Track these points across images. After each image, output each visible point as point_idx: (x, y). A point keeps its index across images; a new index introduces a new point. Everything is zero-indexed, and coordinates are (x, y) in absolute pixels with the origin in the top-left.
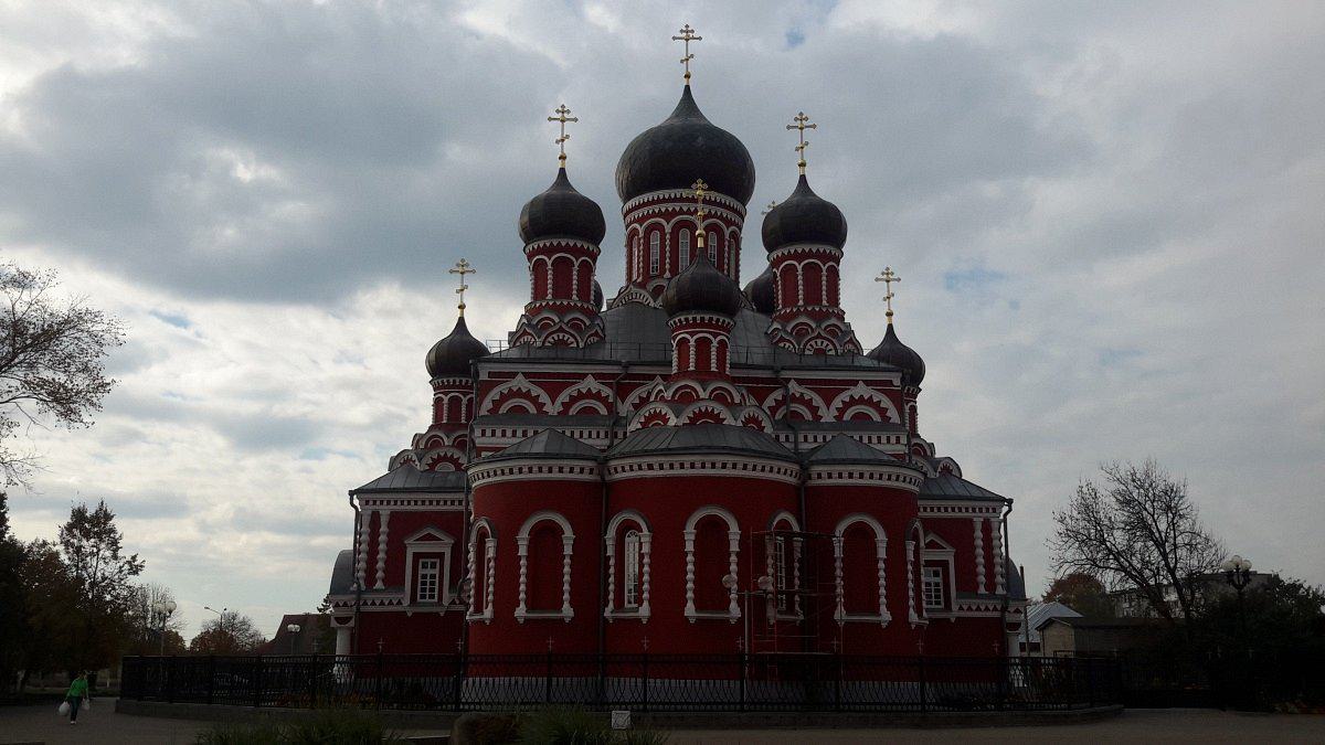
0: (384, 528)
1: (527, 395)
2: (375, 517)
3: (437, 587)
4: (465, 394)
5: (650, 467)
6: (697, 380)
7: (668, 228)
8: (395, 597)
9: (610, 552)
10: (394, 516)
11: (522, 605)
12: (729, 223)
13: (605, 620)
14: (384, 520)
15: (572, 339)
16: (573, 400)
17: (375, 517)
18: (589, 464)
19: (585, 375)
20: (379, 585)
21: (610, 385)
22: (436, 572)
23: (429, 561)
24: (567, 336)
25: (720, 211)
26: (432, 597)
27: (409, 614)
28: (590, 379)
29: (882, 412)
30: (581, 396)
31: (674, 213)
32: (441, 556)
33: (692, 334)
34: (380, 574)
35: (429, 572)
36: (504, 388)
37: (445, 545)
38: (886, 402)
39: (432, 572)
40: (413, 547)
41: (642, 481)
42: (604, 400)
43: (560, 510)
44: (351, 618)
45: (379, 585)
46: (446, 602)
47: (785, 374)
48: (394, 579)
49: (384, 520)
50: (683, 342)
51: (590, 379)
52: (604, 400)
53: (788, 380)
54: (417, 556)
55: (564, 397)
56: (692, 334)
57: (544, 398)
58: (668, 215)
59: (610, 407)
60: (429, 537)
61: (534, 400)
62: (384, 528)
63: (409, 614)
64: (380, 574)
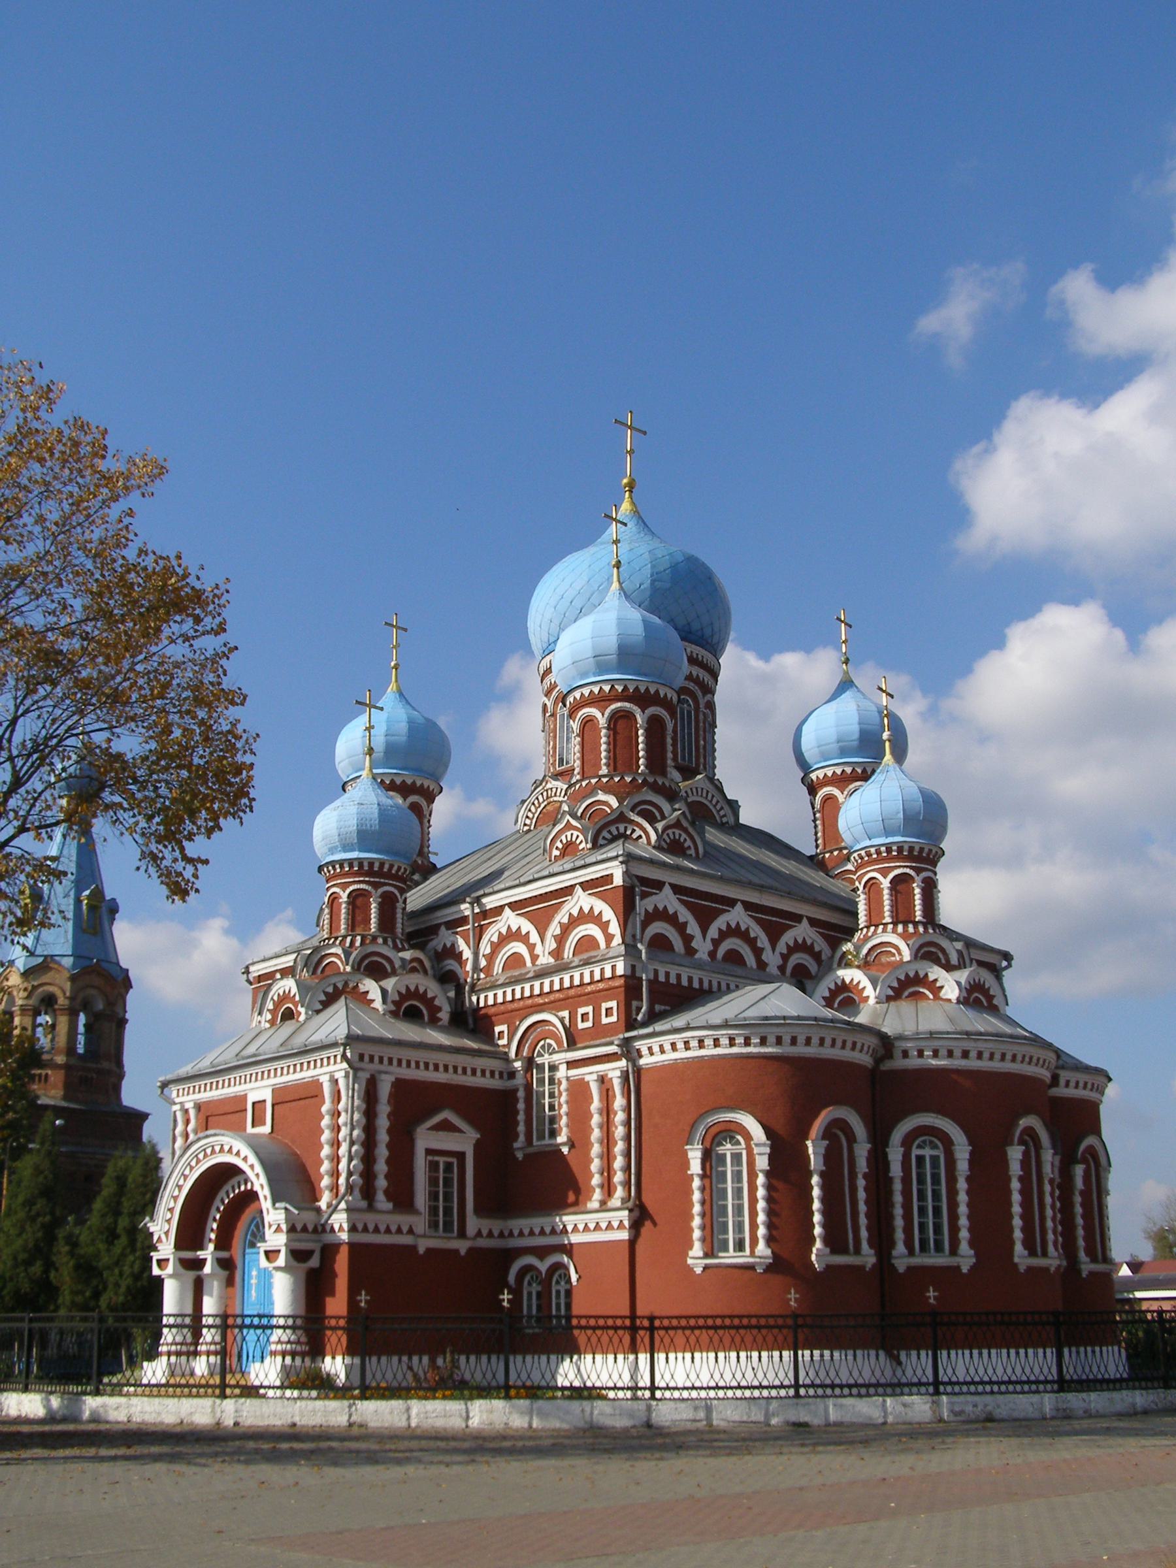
1: (672, 919)
8: (405, 1220)
9: (896, 1170)
10: (400, 1085)
14: (385, 1089)
15: (688, 843)
19: (732, 902)
21: (759, 921)
27: (421, 1250)
28: (739, 907)
34: (381, 1183)
37: (465, 1141)
40: (425, 1139)
45: (382, 1202)
46: (471, 1230)
49: (385, 1089)
51: (739, 907)
56: (884, 872)
57: (693, 928)
59: (757, 952)
60: (446, 1126)
61: (681, 928)
64: (381, 1183)
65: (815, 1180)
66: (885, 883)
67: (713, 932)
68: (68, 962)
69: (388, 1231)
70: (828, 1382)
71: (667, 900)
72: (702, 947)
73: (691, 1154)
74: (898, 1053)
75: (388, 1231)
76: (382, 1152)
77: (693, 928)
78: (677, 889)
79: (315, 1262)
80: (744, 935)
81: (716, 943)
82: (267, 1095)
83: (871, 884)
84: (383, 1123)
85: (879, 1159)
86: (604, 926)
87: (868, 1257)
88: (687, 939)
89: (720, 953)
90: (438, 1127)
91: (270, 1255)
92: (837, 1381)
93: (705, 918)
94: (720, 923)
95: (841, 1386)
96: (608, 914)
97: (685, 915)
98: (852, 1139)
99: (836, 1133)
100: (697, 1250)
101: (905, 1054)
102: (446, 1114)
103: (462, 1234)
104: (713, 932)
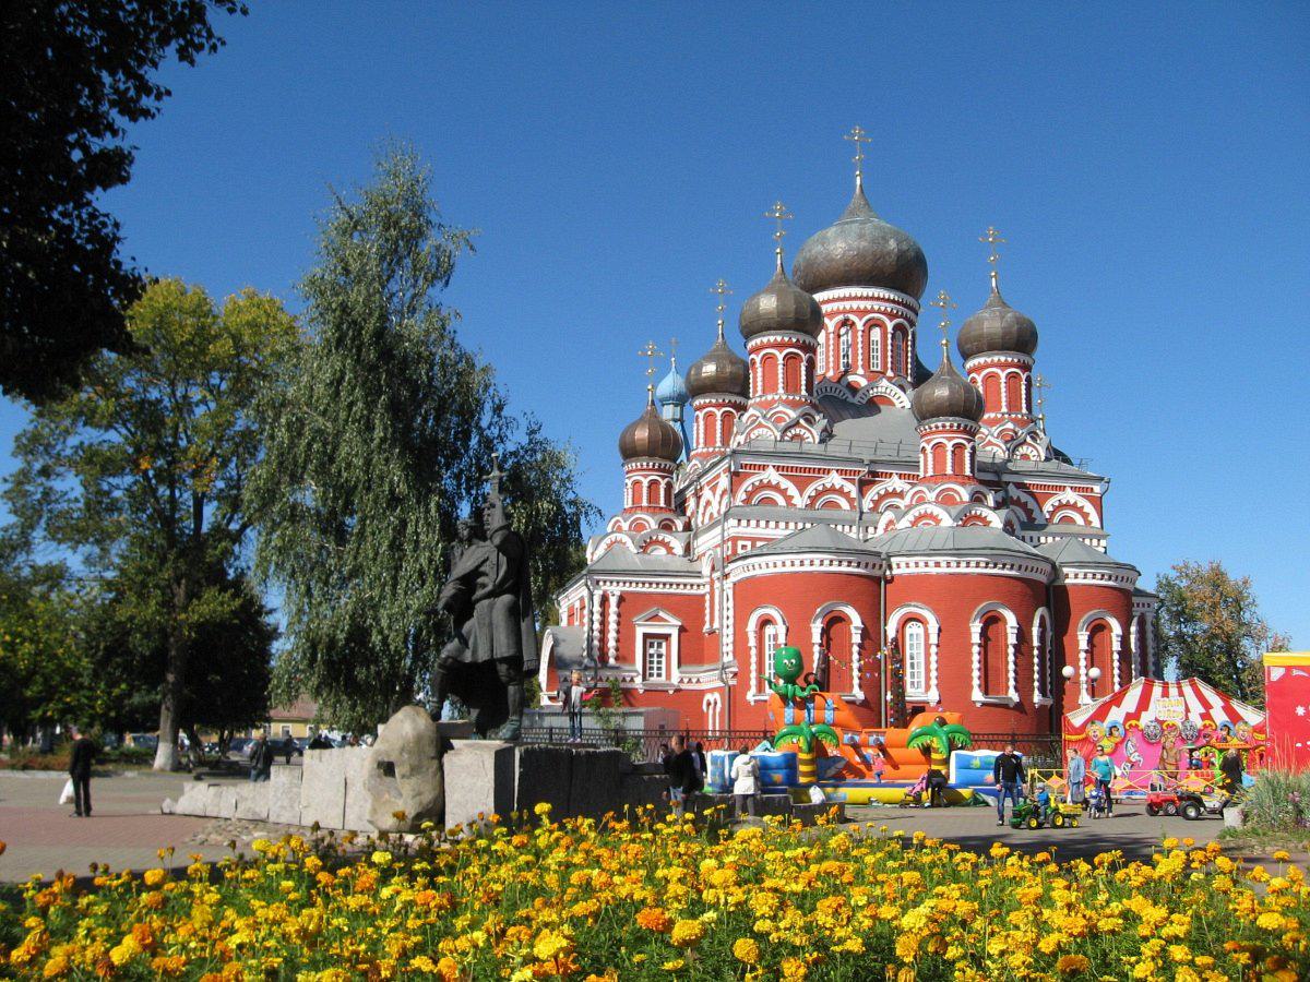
0: (613, 608)
1: (776, 488)
2: (604, 600)
3: (663, 666)
4: (663, 477)
5: (937, 564)
6: (956, 483)
7: (860, 325)
10: (621, 599)
14: (613, 601)
15: (807, 434)
16: (819, 494)
17: (604, 600)
24: (803, 431)
26: (659, 675)
28: (834, 474)
29: (1085, 516)
30: (826, 491)
31: (866, 312)
32: (667, 637)
36: (755, 479)
37: (671, 625)
38: (1089, 508)
41: (928, 577)
47: (1006, 478)
49: (613, 601)
50: (938, 446)
52: (846, 495)
53: (1008, 483)
54: (646, 636)
55: (810, 490)
57: (792, 490)
58: (861, 313)
59: (851, 501)
60: (655, 617)
61: (783, 492)
62: (613, 608)
73: (813, 630)
80: (840, 492)
81: (813, 499)
88: (789, 499)
93: (801, 485)
97: (785, 484)
100: (753, 689)
101: (898, 566)
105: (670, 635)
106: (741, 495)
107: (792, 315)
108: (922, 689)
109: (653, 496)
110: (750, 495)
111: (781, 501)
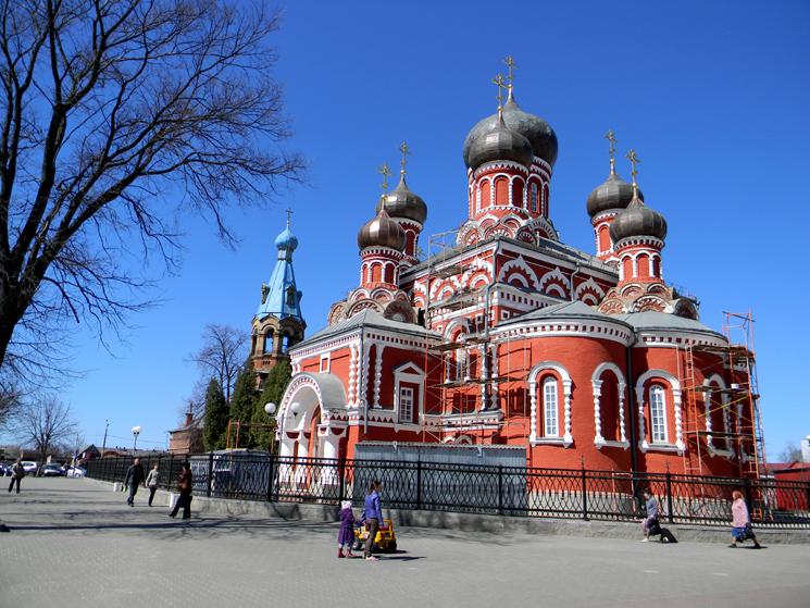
0: (379, 361)
1: (523, 273)
2: (373, 348)
10: (387, 349)
11: (598, 434)
12: (545, 179)
13: (638, 450)
17: (373, 348)
18: (627, 331)
19: (554, 267)
20: (377, 405)
21: (569, 278)
22: (411, 399)
23: (407, 389)
25: (540, 170)
27: (396, 431)
28: (557, 269)
32: (416, 387)
33: (633, 253)
34: (377, 397)
35: (407, 398)
37: (420, 378)
39: (403, 398)
40: (399, 375)
42: (564, 287)
43: (567, 367)
44: (342, 430)
45: (377, 405)
48: (386, 403)
51: (557, 269)
52: (564, 287)
57: (534, 277)
60: (410, 371)
61: (527, 277)
62: (379, 361)
63: (396, 431)
64: (377, 397)
65: (596, 401)
66: (634, 258)
67: (544, 280)
68: (279, 316)
69: (379, 420)
70: (604, 511)
71: (520, 263)
72: (539, 286)
74: (641, 340)
75: (385, 421)
76: (378, 382)
77: (534, 277)
78: (525, 258)
79: (343, 435)
80: (560, 283)
81: (546, 285)
82: (328, 356)
83: (627, 258)
84: (378, 368)
85: (630, 392)
86: (487, 274)
87: (623, 441)
89: (547, 291)
90: (406, 371)
91: (324, 429)
92: (610, 511)
94: (547, 276)
95: (612, 515)
96: (491, 268)
97: (529, 271)
98: (616, 381)
99: (608, 378)
102: (410, 365)
103: (416, 421)
104: (544, 280)
105: (418, 385)
106: (502, 274)
107: (510, 148)
108: (557, 435)
109: (389, 278)
110: (507, 274)
111: (526, 284)
